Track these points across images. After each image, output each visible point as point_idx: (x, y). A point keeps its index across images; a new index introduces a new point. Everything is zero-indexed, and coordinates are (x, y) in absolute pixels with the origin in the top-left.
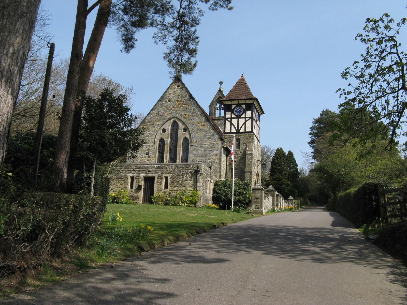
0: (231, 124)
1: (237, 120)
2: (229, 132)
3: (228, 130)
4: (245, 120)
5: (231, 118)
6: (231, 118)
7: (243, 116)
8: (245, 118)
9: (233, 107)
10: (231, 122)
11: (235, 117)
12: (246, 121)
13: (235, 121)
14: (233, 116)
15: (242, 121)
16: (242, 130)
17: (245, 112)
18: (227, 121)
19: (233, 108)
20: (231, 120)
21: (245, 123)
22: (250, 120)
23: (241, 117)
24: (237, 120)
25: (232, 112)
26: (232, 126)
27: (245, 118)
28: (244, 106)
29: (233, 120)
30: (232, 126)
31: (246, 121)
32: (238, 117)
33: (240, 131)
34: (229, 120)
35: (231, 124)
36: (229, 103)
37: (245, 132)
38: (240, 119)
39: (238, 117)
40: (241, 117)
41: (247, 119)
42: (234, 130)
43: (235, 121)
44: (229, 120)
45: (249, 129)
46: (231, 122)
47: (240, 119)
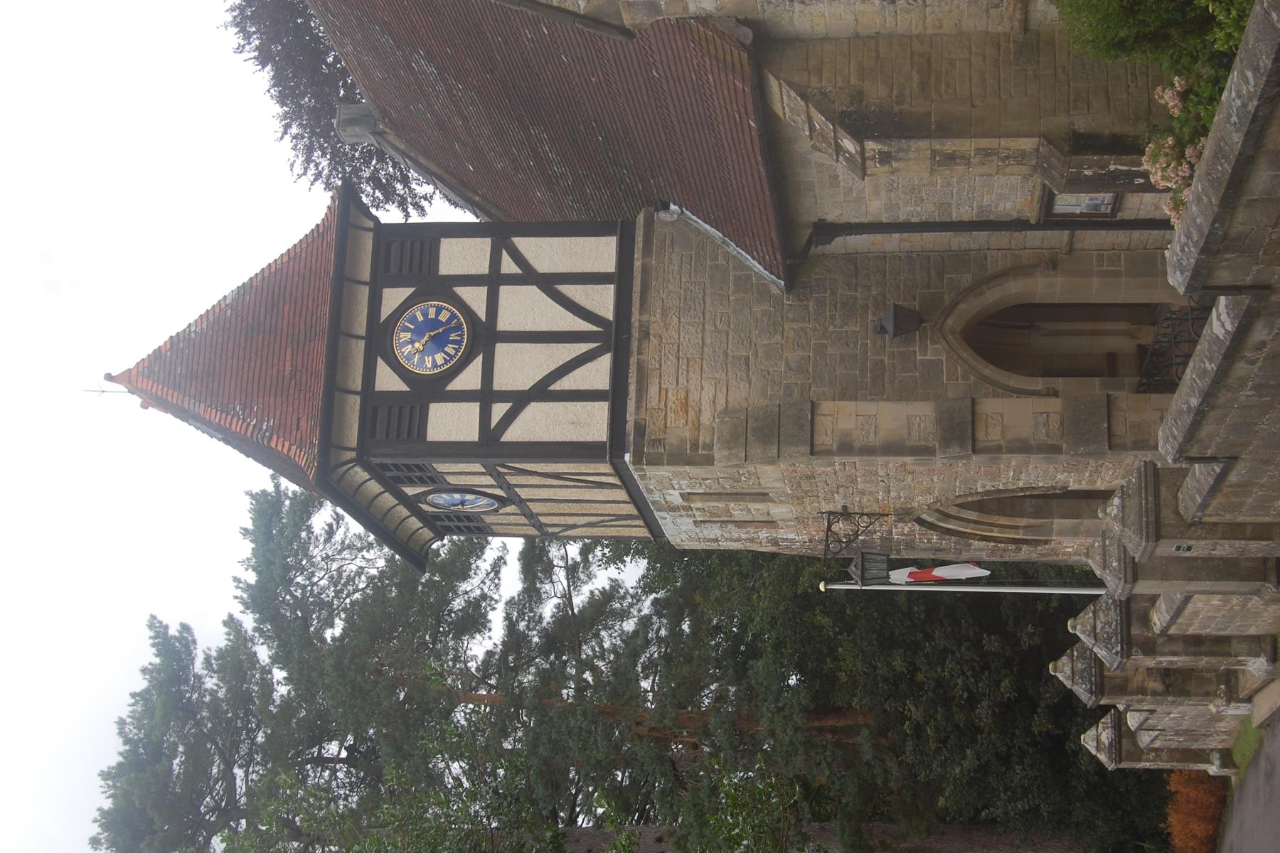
0: (542, 391)
2: (601, 411)
3: (591, 423)
4: (512, 280)
5: (486, 396)
7: (475, 298)
8: (493, 281)
9: (387, 380)
10: (519, 400)
11: (478, 362)
12: (529, 276)
13: (518, 367)
14: (470, 379)
15: (522, 308)
16: (602, 300)
17: (444, 288)
18: (511, 435)
19: (403, 387)
20: (503, 396)
21: (549, 283)
22: (522, 243)
23: (482, 313)
24: (501, 349)
25: (432, 389)
27: (493, 281)
28: (393, 297)
29: (500, 384)
31: (529, 276)
32: (484, 337)
33: (610, 316)
34: (499, 410)
37: (621, 279)
38: (504, 324)
39: (484, 337)
40: (482, 315)
42: (597, 374)
43: (518, 367)
44: (499, 410)
45: (599, 253)
46: (519, 400)
47: (504, 324)
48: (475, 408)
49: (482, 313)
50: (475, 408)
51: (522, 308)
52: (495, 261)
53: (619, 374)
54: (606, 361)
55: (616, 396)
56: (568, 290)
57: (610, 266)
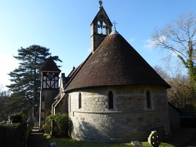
0: (47, 84)
1: (50, 81)
4: (55, 81)
5: (47, 80)
6: (47, 80)
7: (53, 79)
8: (55, 80)
9: (48, 74)
10: (46, 82)
12: (55, 83)
13: (48, 82)
14: (48, 79)
16: (53, 87)
17: (54, 77)
20: (46, 82)
21: (54, 84)
23: (53, 80)
24: (50, 81)
25: (47, 77)
26: (47, 85)
27: (55, 80)
28: (54, 74)
30: (47, 85)
31: (55, 83)
32: (51, 80)
34: (45, 81)
35: (47, 84)
36: (46, 71)
39: (51, 80)
41: (56, 81)
42: (48, 87)
43: (48, 82)
44: (45, 81)
46: (46, 82)
48: (46, 79)
49: (53, 80)
50: (46, 79)
51: (53, 82)
52: (56, 80)
53: (48, 89)
54: (49, 88)
55: (46, 89)
56: (54, 85)
57: (55, 88)
